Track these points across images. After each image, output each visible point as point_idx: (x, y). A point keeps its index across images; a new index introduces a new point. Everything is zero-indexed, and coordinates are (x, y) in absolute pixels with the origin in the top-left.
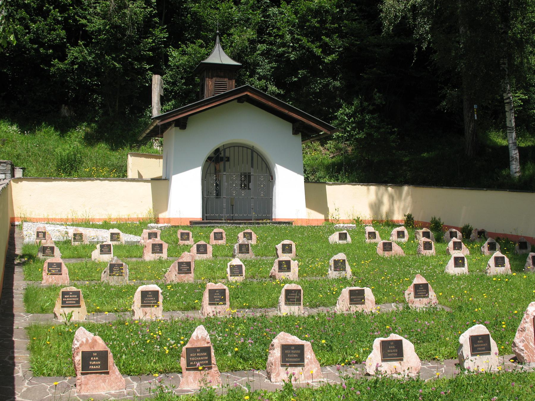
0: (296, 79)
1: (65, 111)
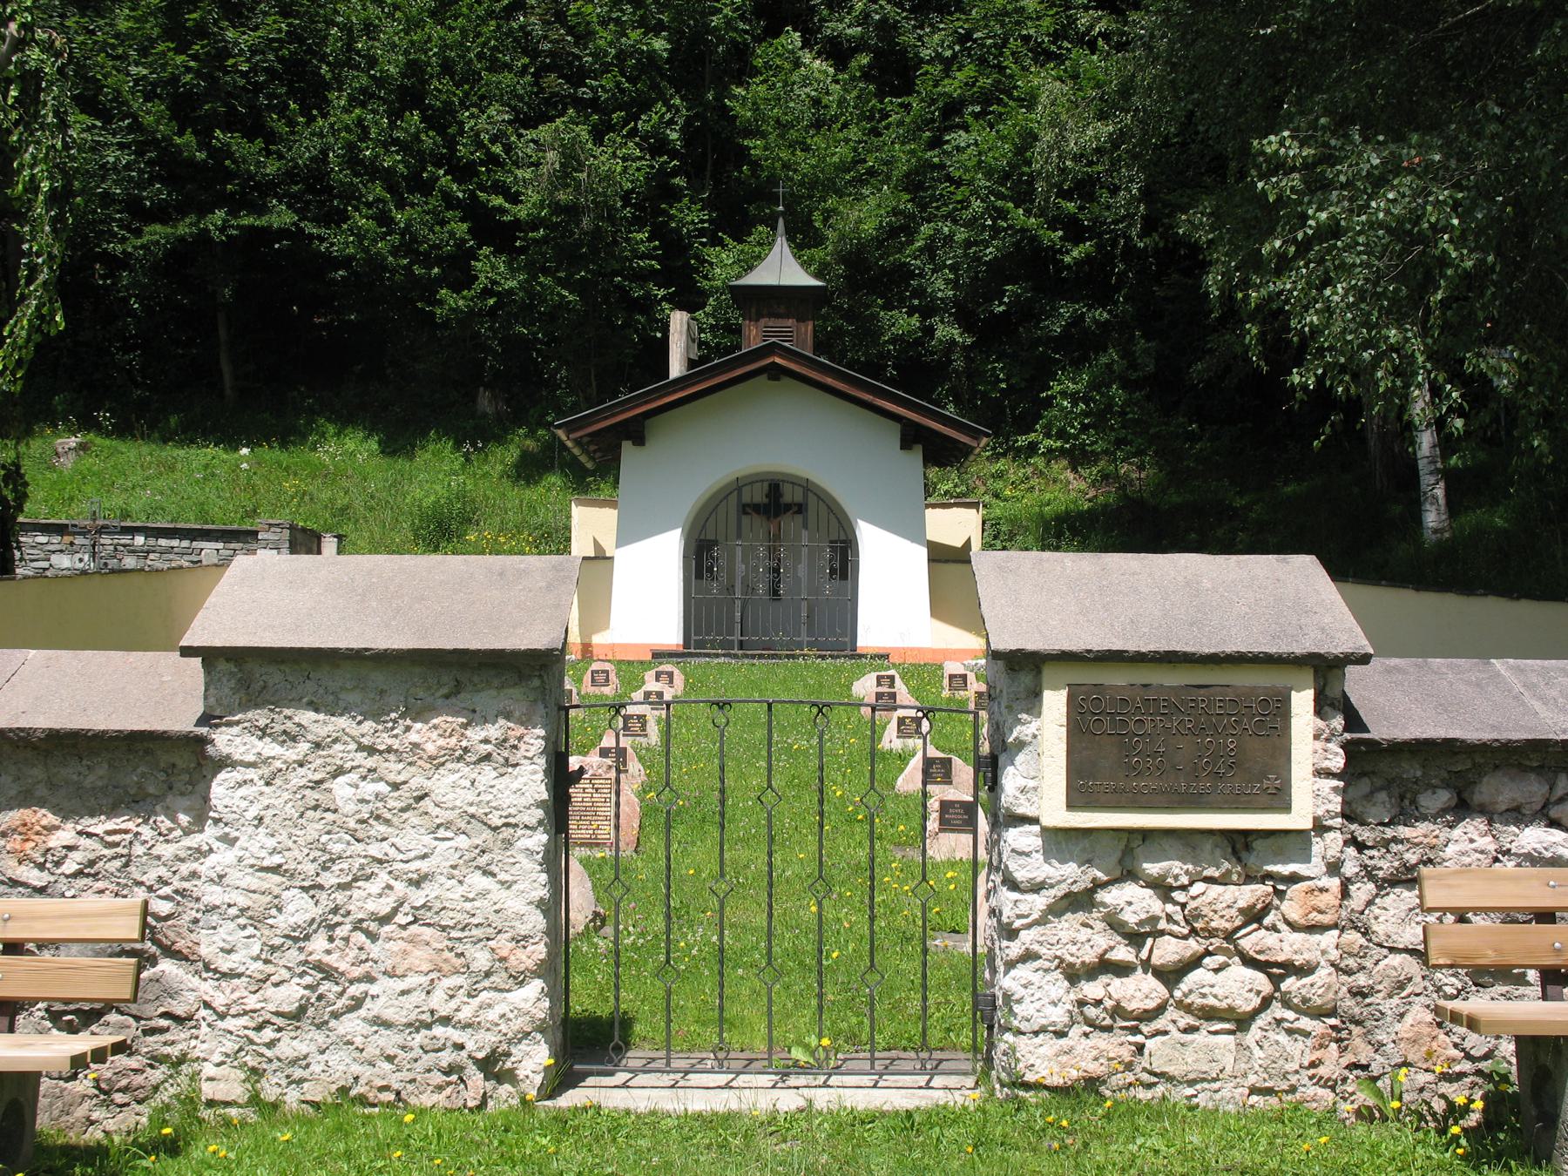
0: (1001, 309)
1: (485, 402)
